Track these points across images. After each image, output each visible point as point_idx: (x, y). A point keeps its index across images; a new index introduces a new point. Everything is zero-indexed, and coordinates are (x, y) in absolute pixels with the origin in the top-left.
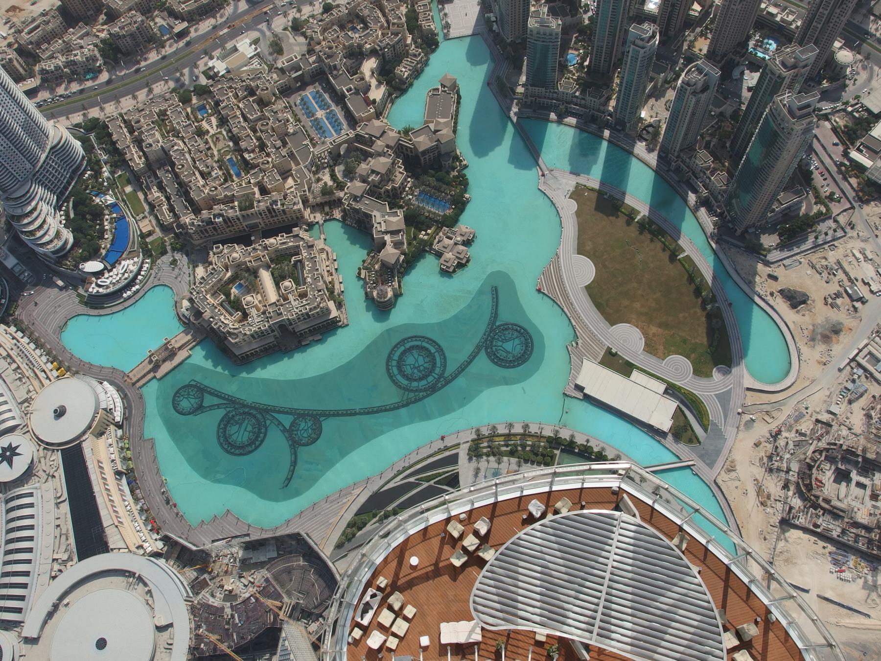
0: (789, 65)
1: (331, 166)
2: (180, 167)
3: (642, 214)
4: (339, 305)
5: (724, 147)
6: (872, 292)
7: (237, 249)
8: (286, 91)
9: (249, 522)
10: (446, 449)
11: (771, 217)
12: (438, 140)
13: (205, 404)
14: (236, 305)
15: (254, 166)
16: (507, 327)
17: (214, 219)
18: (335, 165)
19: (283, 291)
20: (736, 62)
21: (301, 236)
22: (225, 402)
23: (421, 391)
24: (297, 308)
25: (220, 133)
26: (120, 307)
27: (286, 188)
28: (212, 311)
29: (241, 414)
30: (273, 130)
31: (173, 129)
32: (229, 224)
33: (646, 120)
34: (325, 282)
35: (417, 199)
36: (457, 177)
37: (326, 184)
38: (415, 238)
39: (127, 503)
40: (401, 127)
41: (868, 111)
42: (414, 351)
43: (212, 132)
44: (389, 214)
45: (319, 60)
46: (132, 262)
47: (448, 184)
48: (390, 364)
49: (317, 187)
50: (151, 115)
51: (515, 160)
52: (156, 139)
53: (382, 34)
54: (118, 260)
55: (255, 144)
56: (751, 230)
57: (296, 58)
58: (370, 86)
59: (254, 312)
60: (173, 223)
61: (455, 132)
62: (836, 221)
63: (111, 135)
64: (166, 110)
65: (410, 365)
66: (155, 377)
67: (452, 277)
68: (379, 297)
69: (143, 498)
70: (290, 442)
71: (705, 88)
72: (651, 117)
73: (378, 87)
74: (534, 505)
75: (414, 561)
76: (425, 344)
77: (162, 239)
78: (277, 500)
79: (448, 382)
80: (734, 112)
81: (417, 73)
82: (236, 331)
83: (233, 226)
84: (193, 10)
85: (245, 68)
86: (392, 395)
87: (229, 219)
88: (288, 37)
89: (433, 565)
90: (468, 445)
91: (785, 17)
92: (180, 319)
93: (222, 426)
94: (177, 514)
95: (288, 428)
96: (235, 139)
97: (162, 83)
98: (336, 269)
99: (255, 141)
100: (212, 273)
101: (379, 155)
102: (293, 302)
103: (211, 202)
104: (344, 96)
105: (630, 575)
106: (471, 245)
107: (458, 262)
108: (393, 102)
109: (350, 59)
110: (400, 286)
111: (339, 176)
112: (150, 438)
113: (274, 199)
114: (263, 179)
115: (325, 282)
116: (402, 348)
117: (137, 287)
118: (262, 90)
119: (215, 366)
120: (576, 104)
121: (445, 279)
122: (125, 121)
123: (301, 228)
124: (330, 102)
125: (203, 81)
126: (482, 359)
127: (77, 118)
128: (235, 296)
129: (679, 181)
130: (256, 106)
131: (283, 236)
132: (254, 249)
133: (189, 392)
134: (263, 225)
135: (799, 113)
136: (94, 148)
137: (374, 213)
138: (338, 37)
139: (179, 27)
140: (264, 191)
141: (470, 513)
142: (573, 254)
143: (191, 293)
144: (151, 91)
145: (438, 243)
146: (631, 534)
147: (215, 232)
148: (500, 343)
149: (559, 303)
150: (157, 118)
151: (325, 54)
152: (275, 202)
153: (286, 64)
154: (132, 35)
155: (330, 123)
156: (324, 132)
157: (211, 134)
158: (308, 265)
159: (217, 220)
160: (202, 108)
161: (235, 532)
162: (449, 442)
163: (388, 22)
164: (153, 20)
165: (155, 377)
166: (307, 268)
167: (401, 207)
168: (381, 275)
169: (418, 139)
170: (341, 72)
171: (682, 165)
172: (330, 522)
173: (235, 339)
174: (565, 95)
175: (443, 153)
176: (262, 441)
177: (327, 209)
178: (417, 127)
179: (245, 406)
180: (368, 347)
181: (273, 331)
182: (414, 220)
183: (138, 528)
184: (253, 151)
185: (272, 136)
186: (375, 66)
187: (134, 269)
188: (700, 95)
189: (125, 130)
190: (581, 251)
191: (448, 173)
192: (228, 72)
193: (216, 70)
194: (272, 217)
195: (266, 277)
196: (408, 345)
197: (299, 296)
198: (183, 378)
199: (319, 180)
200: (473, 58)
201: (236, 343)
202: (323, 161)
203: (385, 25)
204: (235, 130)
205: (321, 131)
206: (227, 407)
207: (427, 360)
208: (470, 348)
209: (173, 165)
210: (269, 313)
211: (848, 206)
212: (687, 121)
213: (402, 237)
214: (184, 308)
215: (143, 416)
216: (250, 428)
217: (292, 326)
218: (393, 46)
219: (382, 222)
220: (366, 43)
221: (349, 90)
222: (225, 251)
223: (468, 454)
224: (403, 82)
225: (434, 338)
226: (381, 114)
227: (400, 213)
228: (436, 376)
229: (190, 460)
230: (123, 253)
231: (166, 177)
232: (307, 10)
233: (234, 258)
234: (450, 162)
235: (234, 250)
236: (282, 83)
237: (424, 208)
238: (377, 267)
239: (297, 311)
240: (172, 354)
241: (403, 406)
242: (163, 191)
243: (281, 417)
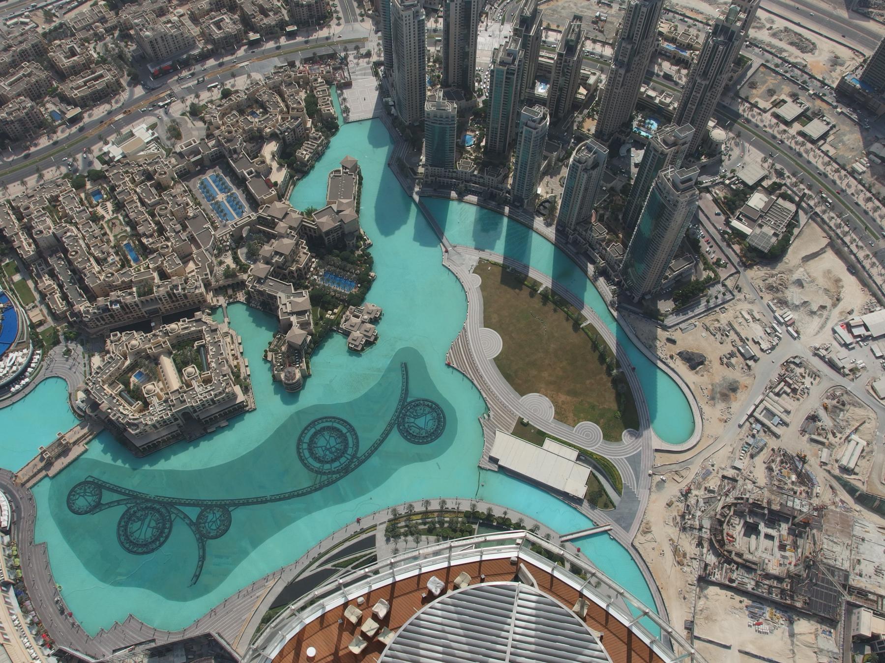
0: (670, 142)
1: (233, 249)
2: (73, 253)
3: (544, 286)
4: (246, 389)
5: (616, 219)
6: (762, 350)
7: (136, 336)
8: (185, 175)
9: (155, 626)
10: (363, 531)
11: (665, 283)
12: (341, 221)
13: (103, 502)
14: (135, 395)
15: (153, 251)
16: (419, 403)
17: (111, 306)
18: (238, 247)
19: (186, 378)
20: (622, 141)
21: (203, 320)
22: (126, 497)
23: (334, 473)
24: (201, 395)
25: (117, 218)
26: (8, 402)
27: (187, 272)
28: (110, 402)
29: (143, 509)
30: (172, 214)
31: (66, 215)
32: (127, 310)
33: (542, 196)
34: (230, 366)
35: (322, 279)
36: (362, 256)
37: (228, 266)
38: (322, 318)
39: (14, 617)
40: (303, 208)
41: (743, 183)
42: (326, 433)
43: (108, 217)
44: (295, 295)
45: (219, 144)
46: (21, 353)
47: (352, 264)
48: (301, 447)
49: (219, 270)
50: (41, 201)
51: (420, 238)
52: (47, 226)
53: (283, 119)
54: (5, 353)
55: (153, 229)
56: (647, 297)
57: (195, 142)
58: (271, 169)
59: (155, 401)
60: (66, 311)
61: (358, 211)
62: (724, 285)
64: (58, 196)
65: (321, 447)
66: (47, 476)
67: (361, 356)
68: (286, 379)
69: (34, 610)
70: (198, 536)
71: (595, 165)
72: (547, 193)
73: (279, 170)
74: (434, 582)
75: (311, 652)
76: (336, 425)
77: (54, 328)
78: (185, 599)
79: (361, 462)
80: (623, 187)
81: (318, 156)
82: (136, 422)
83: (131, 312)
84: (86, 96)
85: (142, 153)
86: (305, 480)
87: (126, 305)
88: (187, 122)
89: (333, 654)
90: (384, 526)
91: (663, 100)
92: (75, 411)
93: (123, 523)
94: (73, 624)
95: (194, 521)
96: (133, 224)
97: (54, 168)
98: (242, 353)
99: (153, 225)
100: (109, 362)
101: (280, 236)
102: (197, 389)
103: (107, 289)
104: (244, 179)
105: (533, 647)
106: (379, 323)
107: (366, 340)
108: (294, 184)
109: (250, 143)
110: (308, 367)
111: (242, 259)
112: (41, 542)
113: (175, 283)
114: (162, 263)
115: (230, 366)
116: (313, 431)
117: (27, 380)
118: (160, 174)
119: (115, 460)
120: (475, 183)
121: (354, 357)
122: (13, 208)
123: (203, 312)
124: (231, 185)
125: (98, 166)
126: (395, 437)
128: (135, 385)
129: (577, 253)
130: (154, 191)
131: (185, 321)
132: (154, 335)
133: (85, 490)
134: (163, 310)
135: (682, 186)
138: (237, 121)
139: (72, 112)
140: (163, 276)
141: (368, 596)
142: (480, 327)
143: (87, 384)
144: (41, 177)
145: (346, 321)
146: (533, 605)
147: (112, 320)
148: (412, 420)
149: (469, 376)
150: (48, 204)
152: (176, 287)
153: (185, 148)
154: (21, 121)
155: (232, 206)
156: (225, 215)
159: (114, 307)
160: (97, 193)
161: (139, 638)
162: (365, 524)
163: (287, 106)
164: (44, 105)
165: (47, 476)
166: (211, 353)
167: (306, 288)
168: (288, 357)
169: (321, 220)
170: (241, 156)
171: (579, 238)
172: (243, 618)
173: (136, 430)
174: (464, 174)
176: (167, 537)
177: (230, 292)
178: (320, 208)
179: (148, 500)
180: (278, 432)
181: (176, 419)
182: (320, 300)
183: (28, 644)
184: (151, 236)
186: (275, 149)
187: (24, 361)
188: (591, 172)
189: (13, 217)
190: (487, 323)
191: (353, 252)
192: (124, 157)
193: (111, 155)
194: (173, 302)
195: (167, 364)
196: (318, 427)
197: (203, 382)
198: (79, 474)
199: (221, 263)
200: (375, 141)
201: (136, 434)
202: (225, 244)
203: (285, 109)
204: (132, 215)
205: (222, 214)
206: (127, 503)
207: (339, 440)
208: (381, 426)
209: (65, 251)
210: (172, 401)
211: (734, 270)
212: (580, 196)
213: (308, 317)
214: (79, 400)
215: (34, 519)
216: (153, 524)
217: (197, 414)
218: (294, 130)
219: (288, 303)
220: (266, 127)
221: (250, 173)
222: (124, 339)
223: (385, 535)
224: (304, 164)
225: (344, 418)
226: (283, 196)
227: (306, 294)
228: (349, 457)
229: (87, 564)
230: (11, 345)
231: (57, 264)
232: (205, 96)
233: (133, 346)
234: (354, 241)
235: (133, 337)
236: (180, 168)
237: (329, 288)
238: (283, 348)
239: (202, 397)
240: (65, 450)
241: (316, 490)
242: (55, 278)
243: (186, 510)
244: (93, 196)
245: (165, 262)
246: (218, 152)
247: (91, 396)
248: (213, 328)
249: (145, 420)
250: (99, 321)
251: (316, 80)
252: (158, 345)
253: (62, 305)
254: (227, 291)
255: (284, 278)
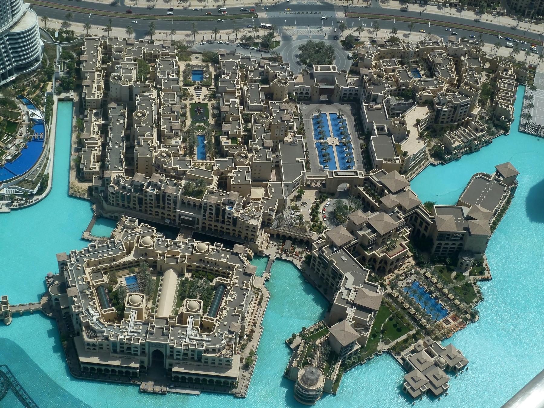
2: (140, 115)
4: (246, 367)
12: (467, 229)
17: (148, 187)
21: (242, 257)
24: (191, 339)
30: (270, 127)
31: (154, 77)
32: (161, 204)
37: (301, 218)
43: (196, 100)
45: (361, 83)
53: (447, 90)
55: (240, 132)
58: (408, 135)
59: (133, 316)
60: (96, 173)
61: (493, 228)
63: (80, 53)
64: (157, 56)
68: (302, 379)
83: (164, 208)
87: (164, 197)
96: (220, 118)
99: (242, 129)
100: (108, 246)
101: (385, 210)
102: (189, 330)
110: (337, 380)
113: (232, 198)
115: (243, 328)
121: (402, 401)
127: (55, 24)
128: (121, 287)
130: (262, 95)
132: (175, 243)
134: (200, 226)
136: (55, 58)
137: (347, 275)
140: (223, 184)
143: (70, 256)
147: (137, 206)
150: (142, 56)
151: (370, 80)
152: (231, 203)
153: (319, 71)
156: (329, 159)
157: (193, 102)
158: (232, 295)
159: (149, 190)
160: (199, 72)
163: (460, 81)
166: (229, 298)
173: (91, 338)
175: (466, 247)
177: (288, 243)
181: (143, 353)
184: (234, 139)
185: (265, 132)
189: (100, 56)
197: (201, 326)
201: (88, 344)
204: (224, 108)
209: (132, 110)
210: (153, 327)
218: (456, 107)
221: (381, 129)
222: (139, 230)
224: (448, 150)
227: (381, 293)
236: (304, 88)
242: (104, 135)
244: (193, 74)
245: (233, 171)
246: (354, 93)
247: (65, 273)
248: (247, 271)
249: (109, 331)
250: (123, 200)
251: (506, 70)
252: (174, 257)
253: (94, 164)
254: (284, 243)
255: (363, 260)
